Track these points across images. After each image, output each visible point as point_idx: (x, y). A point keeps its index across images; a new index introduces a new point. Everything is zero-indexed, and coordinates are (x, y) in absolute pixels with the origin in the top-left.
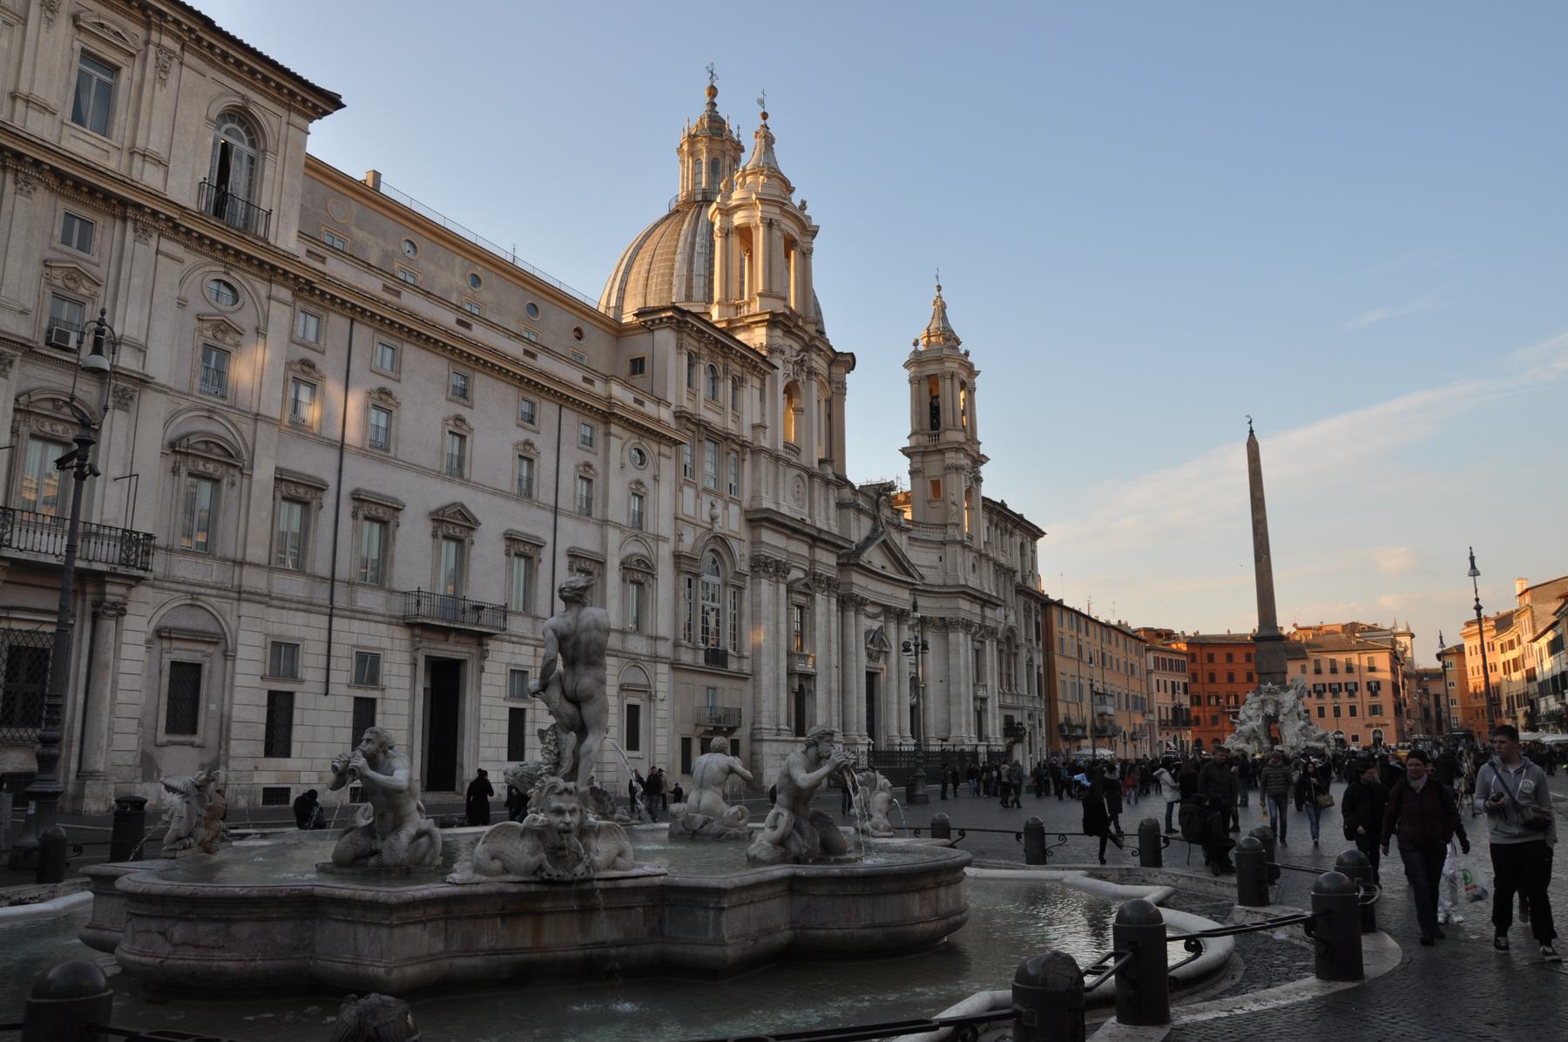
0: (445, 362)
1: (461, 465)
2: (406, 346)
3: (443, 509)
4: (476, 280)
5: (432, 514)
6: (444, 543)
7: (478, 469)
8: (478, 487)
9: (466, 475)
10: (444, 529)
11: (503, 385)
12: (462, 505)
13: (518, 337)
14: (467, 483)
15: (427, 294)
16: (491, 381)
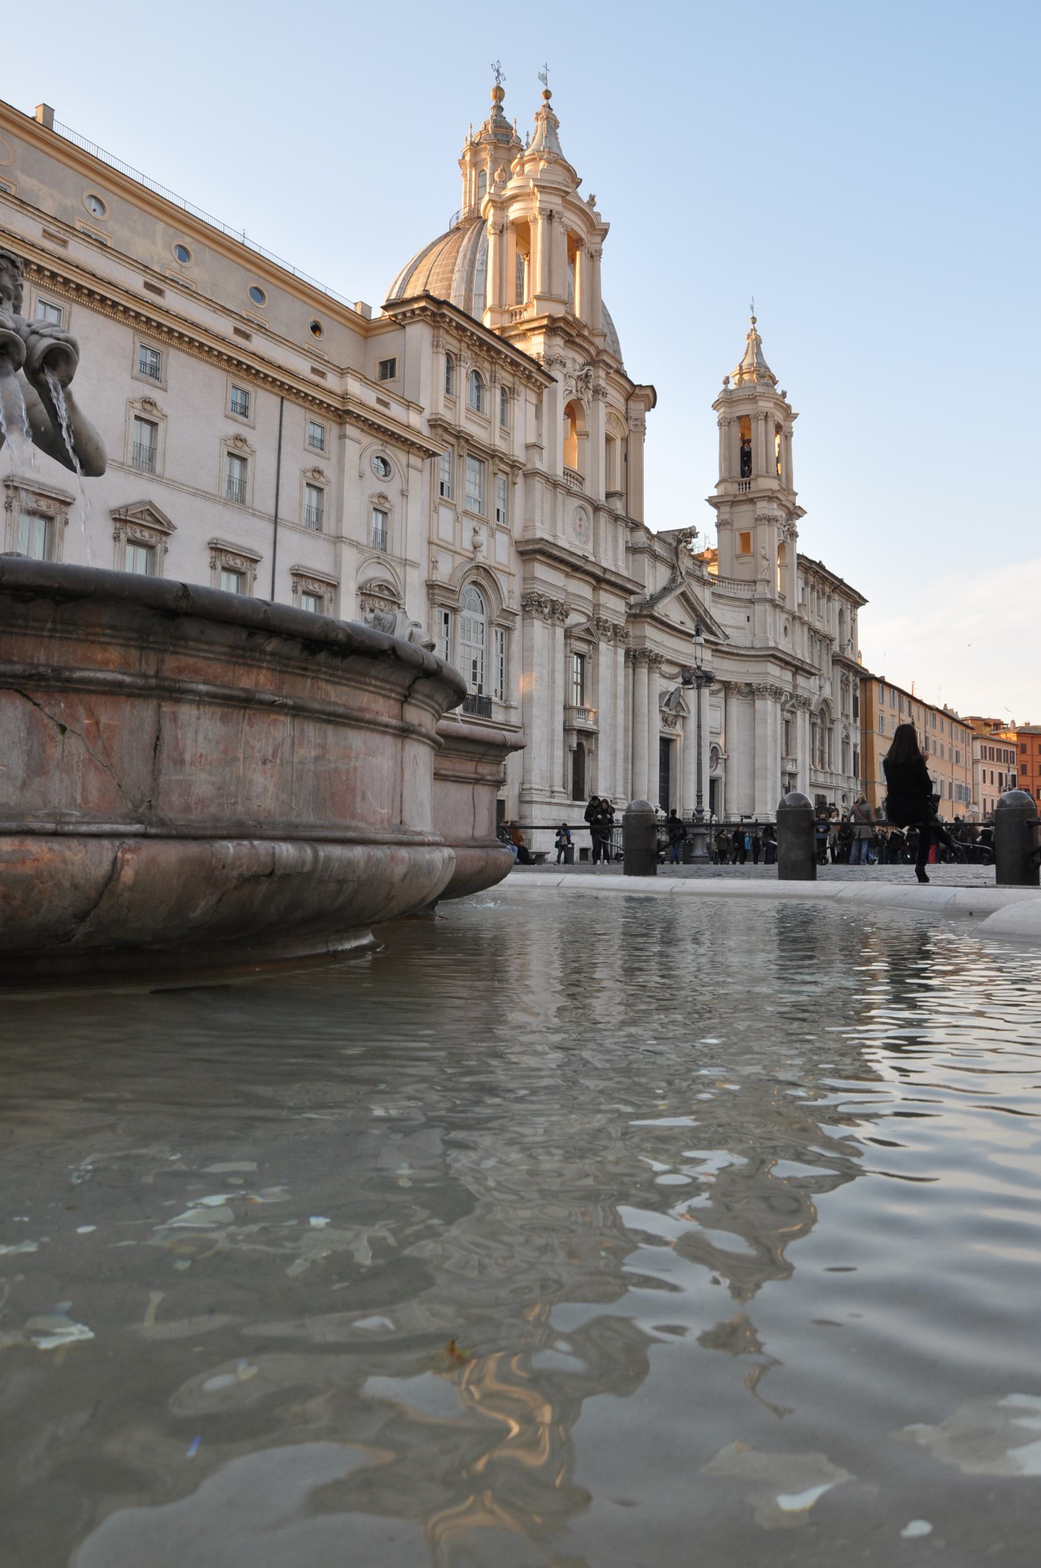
0: (130, 332)
1: (152, 458)
2: (76, 308)
3: (127, 508)
4: (184, 253)
5: (112, 512)
6: (130, 549)
7: (170, 465)
8: (172, 485)
9: (159, 469)
10: (129, 531)
11: (206, 367)
12: (151, 503)
13: (226, 311)
14: (158, 479)
15: (103, 245)
16: (193, 360)
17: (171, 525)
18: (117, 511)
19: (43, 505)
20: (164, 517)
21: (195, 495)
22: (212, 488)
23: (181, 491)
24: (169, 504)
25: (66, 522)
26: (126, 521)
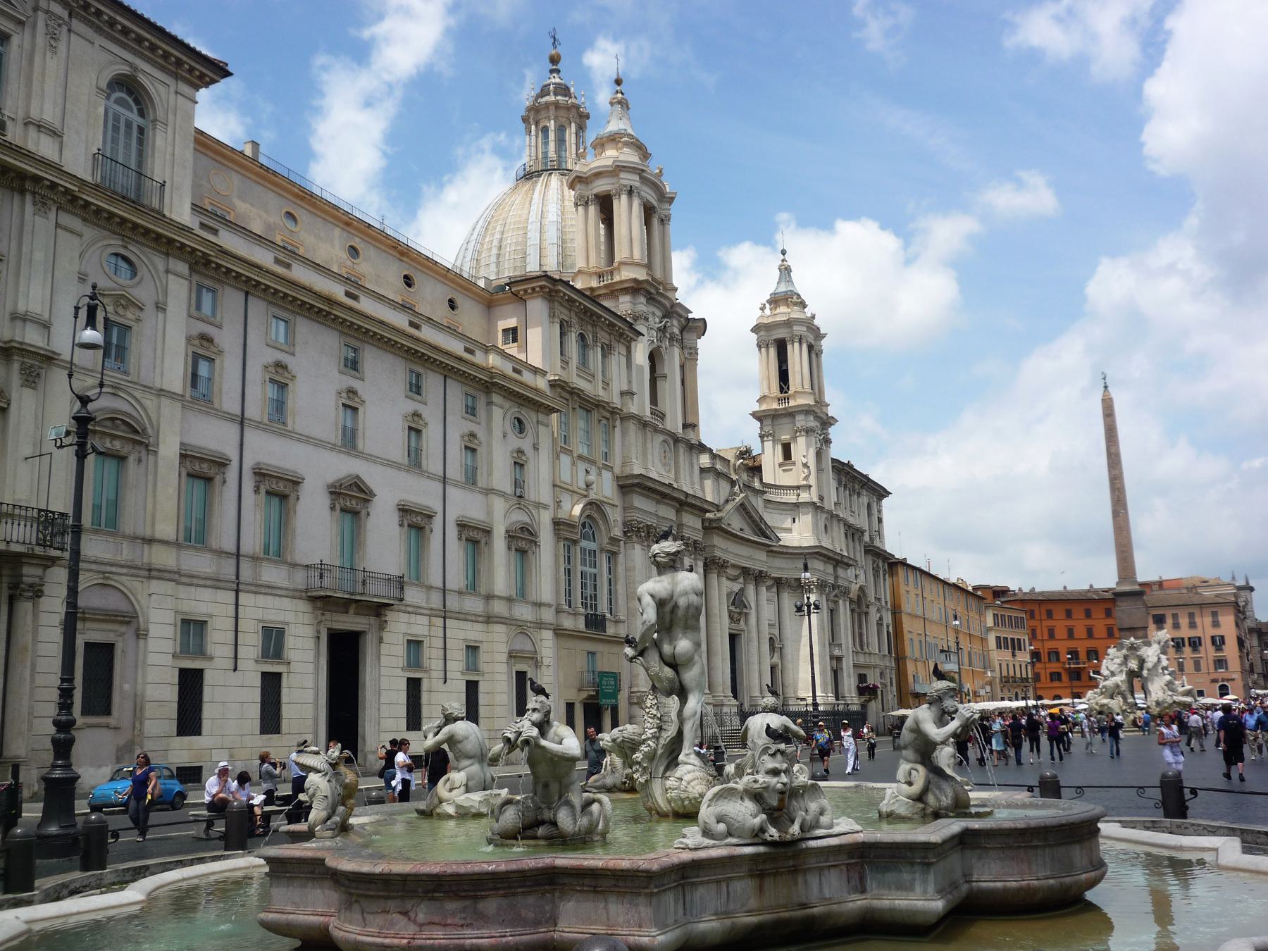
7: (368, 442)
8: (370, 458)
9: (360, 446)
12: (358, 477)
14: (361, 455)
17: (372, 494)
18: (332, 485)
19: (281, 487)
20: (367, 487)
21: (386, 465)
22: (400, 461)
23: (377, 463)
24: (372, 476)
25: (298, 499)
26: (340, 494)
